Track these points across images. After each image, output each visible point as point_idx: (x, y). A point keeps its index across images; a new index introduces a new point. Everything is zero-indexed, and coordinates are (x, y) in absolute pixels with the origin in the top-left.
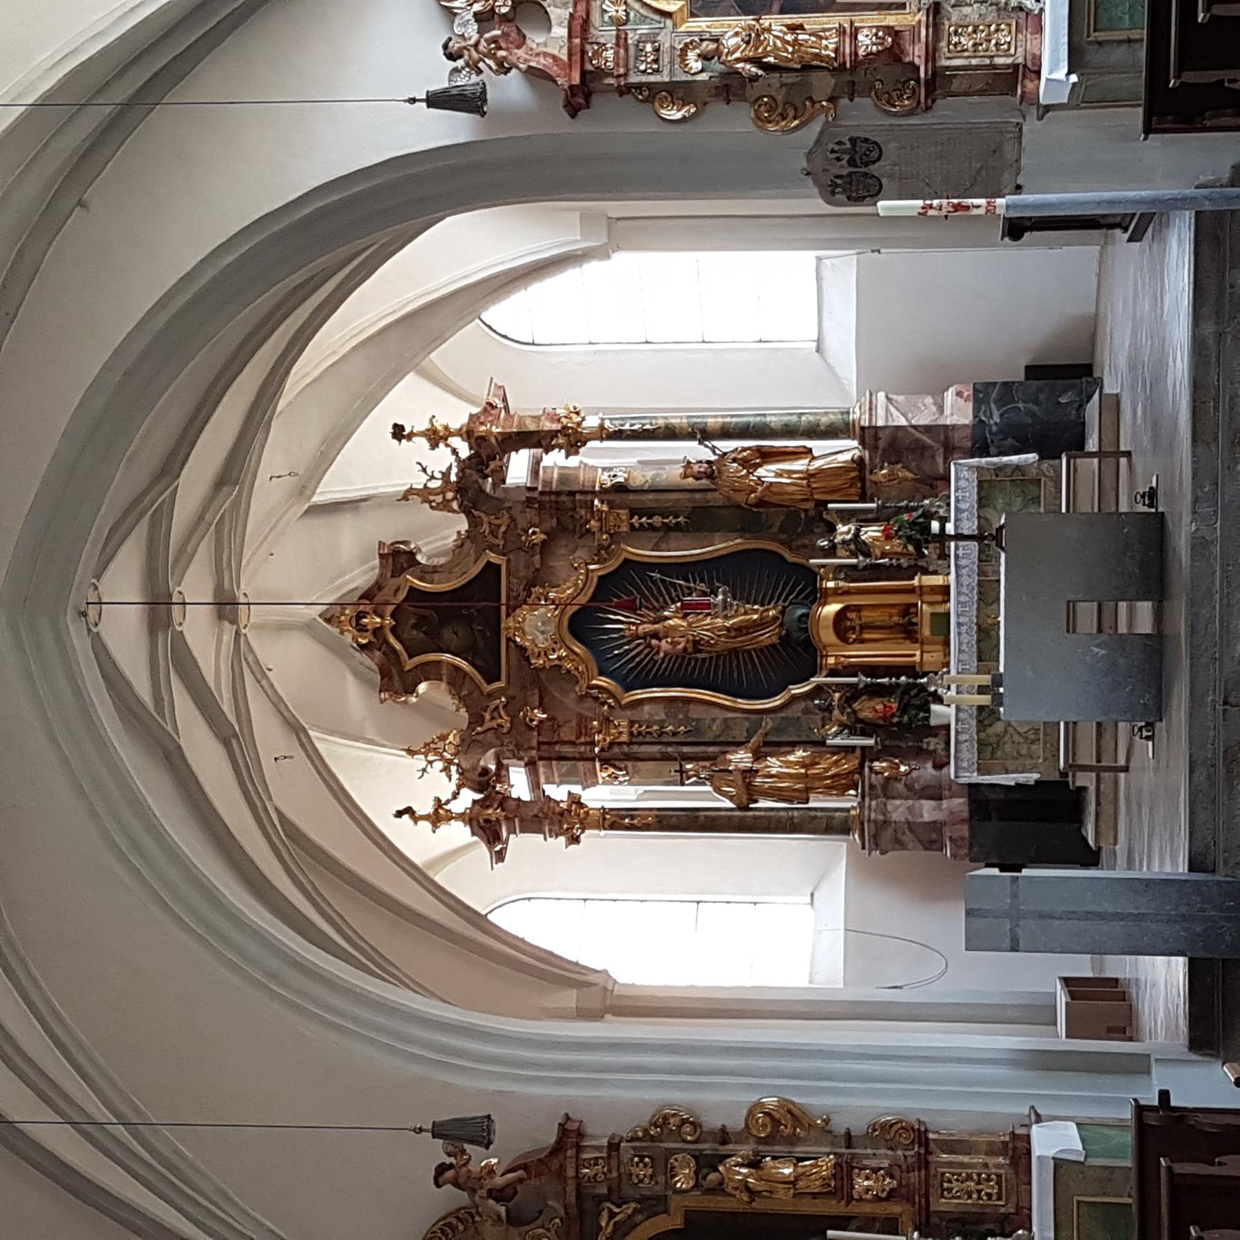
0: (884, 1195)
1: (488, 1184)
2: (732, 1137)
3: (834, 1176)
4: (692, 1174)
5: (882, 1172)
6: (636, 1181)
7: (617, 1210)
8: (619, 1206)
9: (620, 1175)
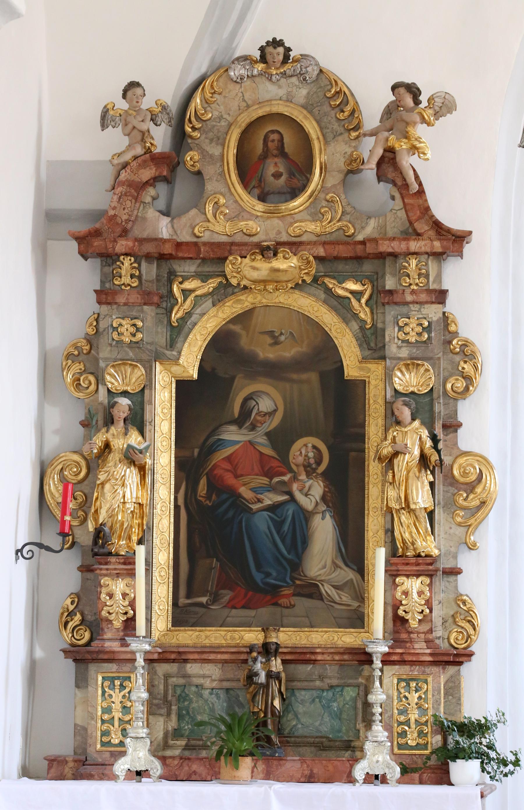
0: (401, 612)
1: (402, 146)
2: (451, 435)
3: (419, 556)
4: (411, 389)
5: (428, 611)
6: (401, 324)
7: (363, 301)
8: (366, 304)
9: (407, 303)
